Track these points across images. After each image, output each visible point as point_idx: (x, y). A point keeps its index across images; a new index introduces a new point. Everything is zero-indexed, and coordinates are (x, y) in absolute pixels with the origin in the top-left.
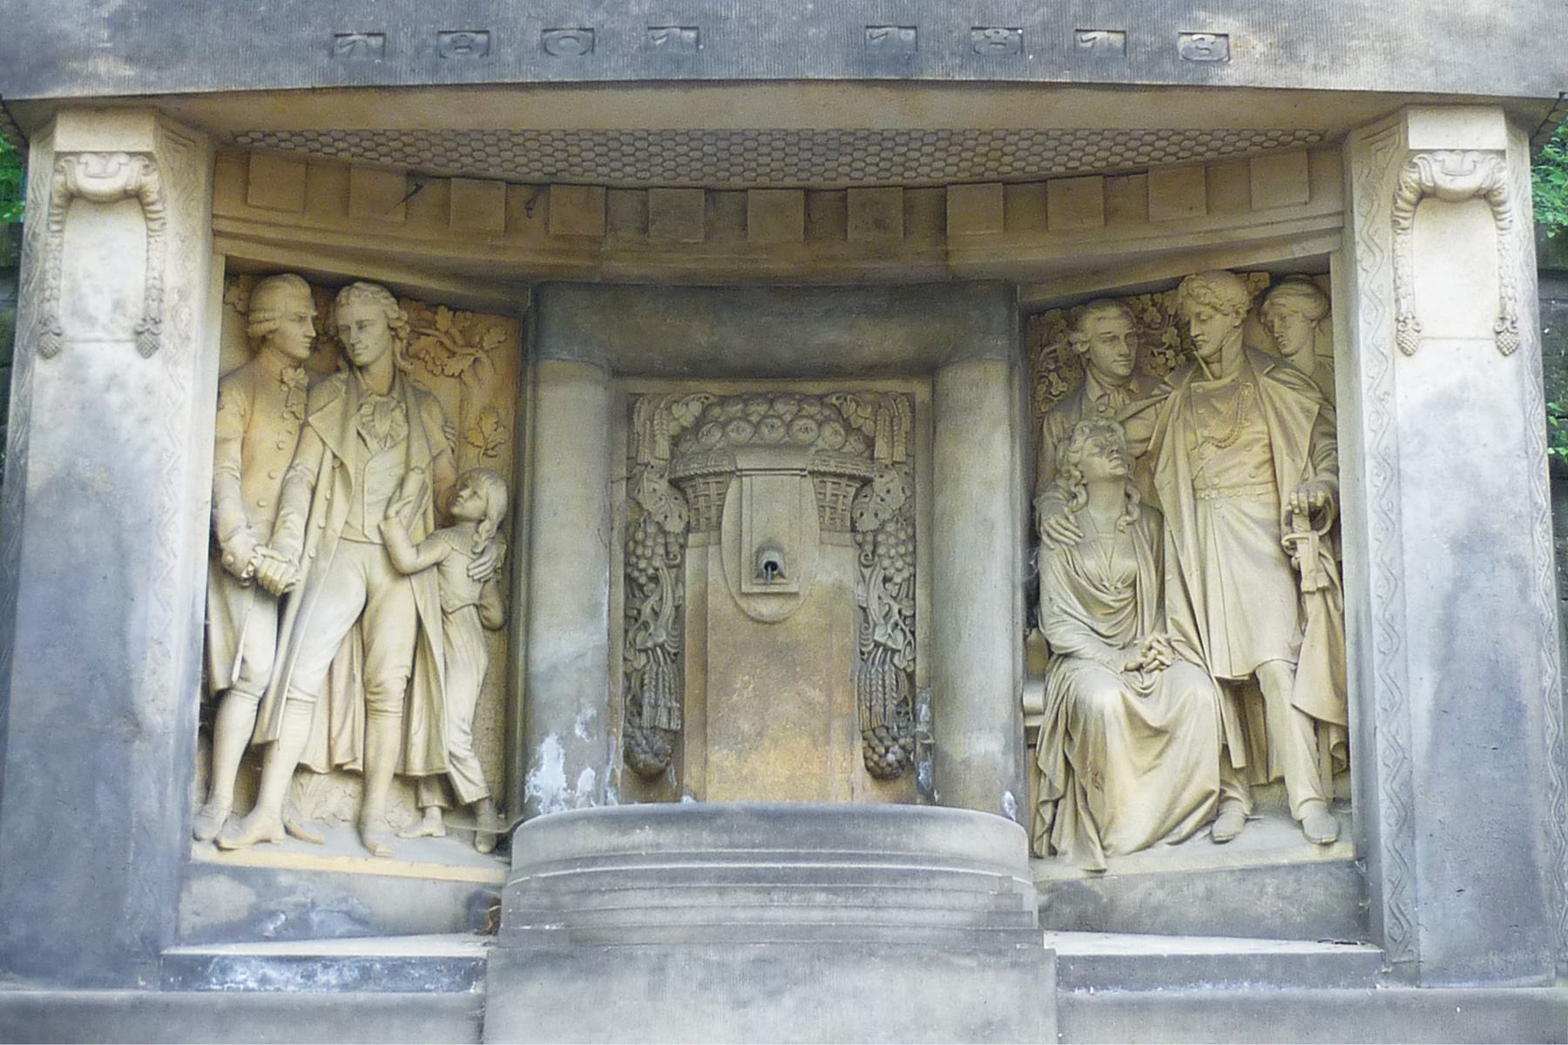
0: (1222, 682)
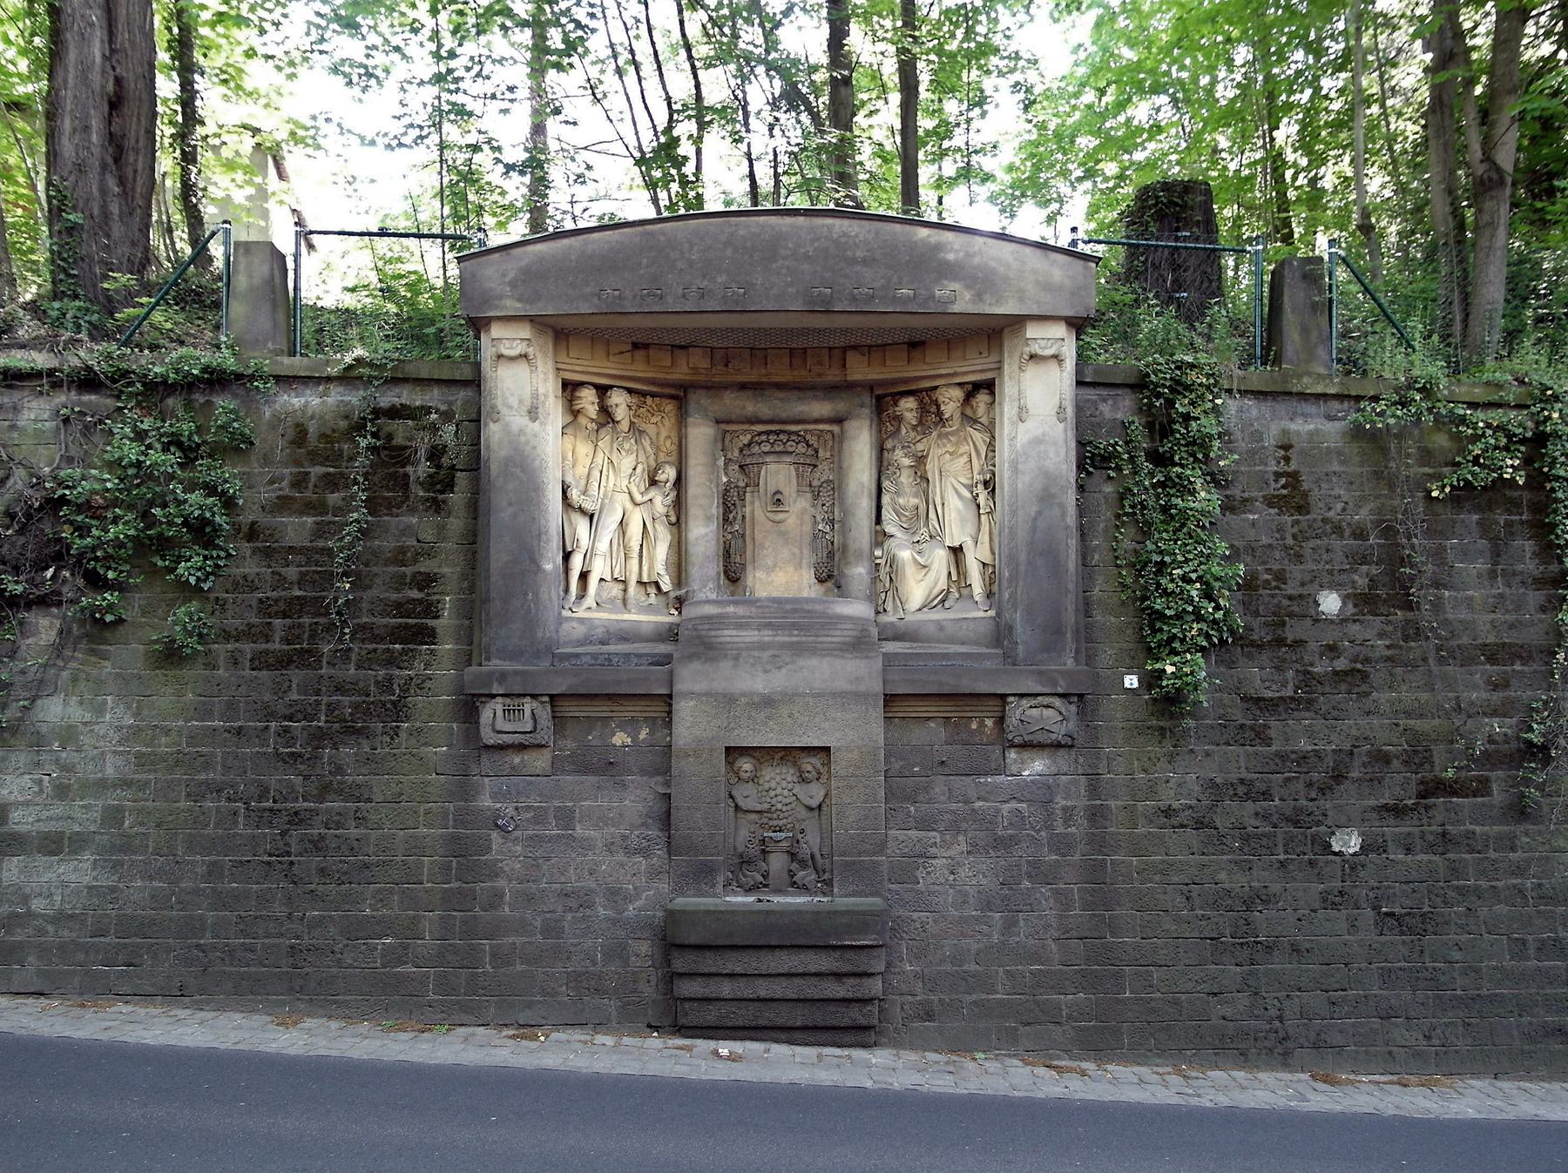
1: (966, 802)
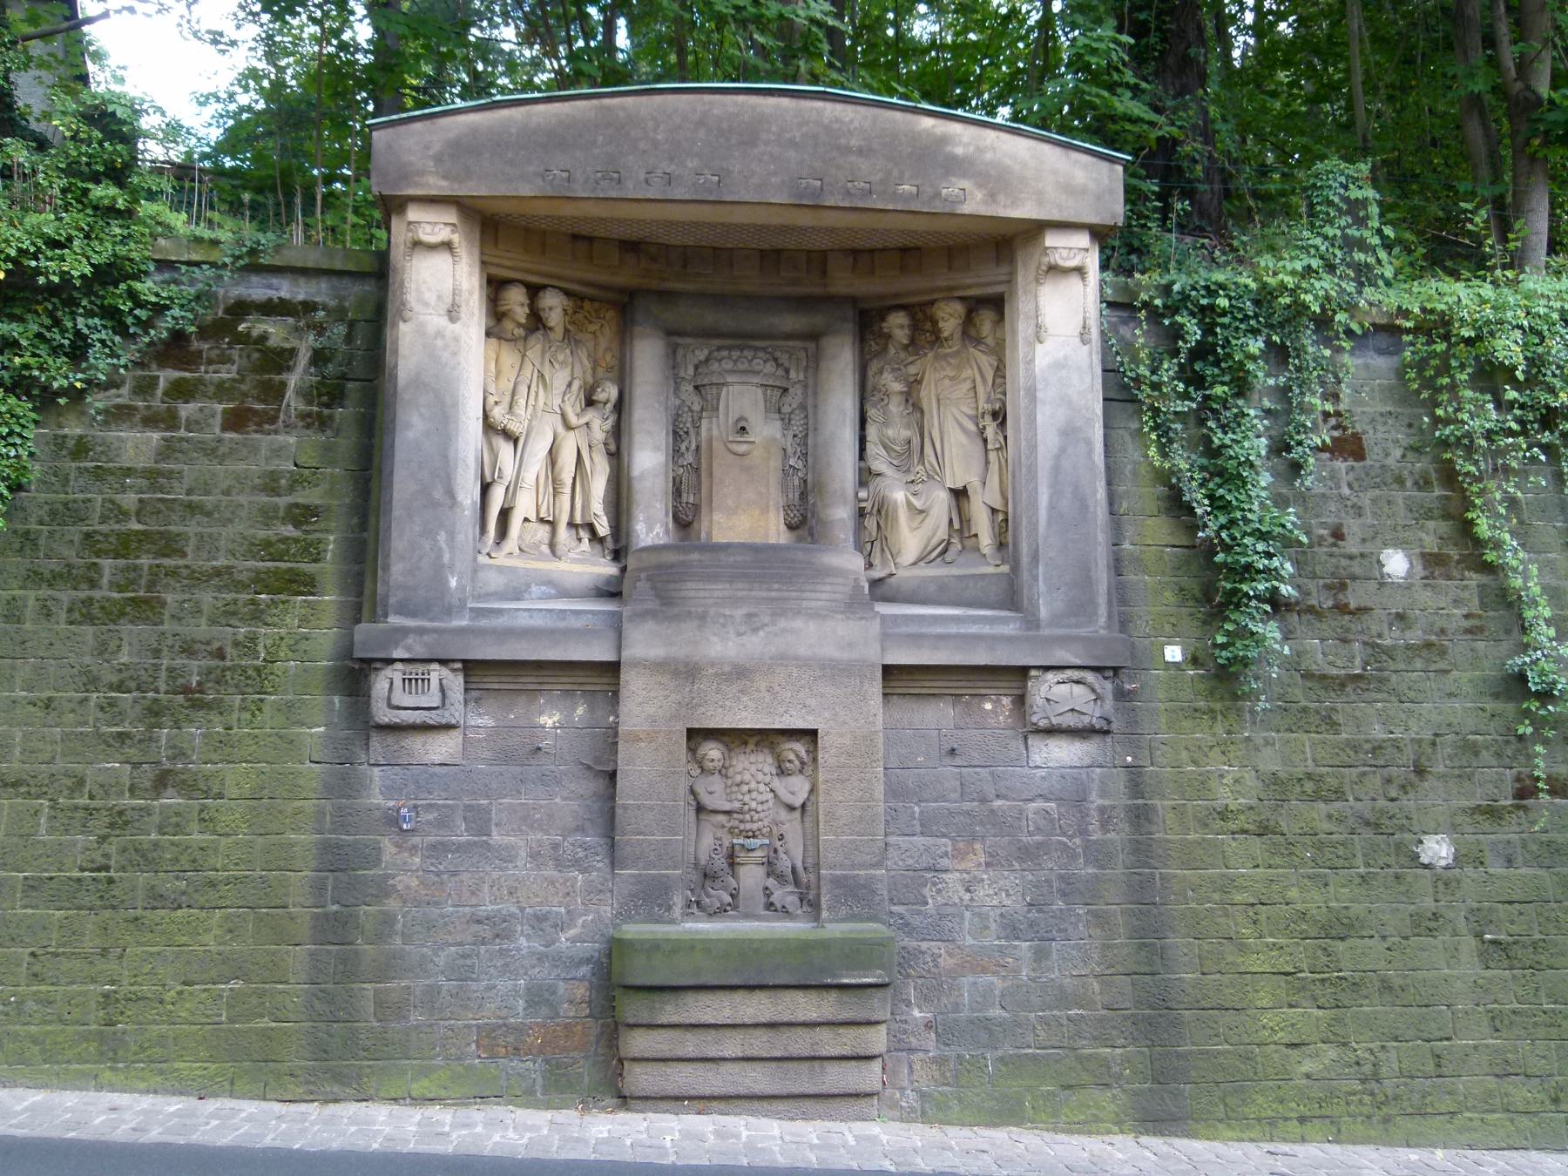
0: (951, 490)
1: (984, 800)
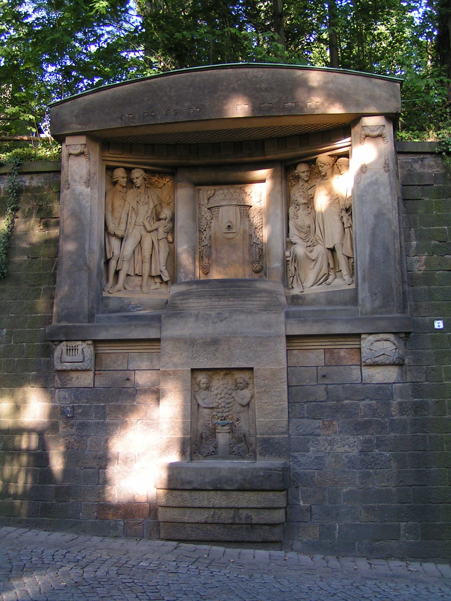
0: (328, 249)
